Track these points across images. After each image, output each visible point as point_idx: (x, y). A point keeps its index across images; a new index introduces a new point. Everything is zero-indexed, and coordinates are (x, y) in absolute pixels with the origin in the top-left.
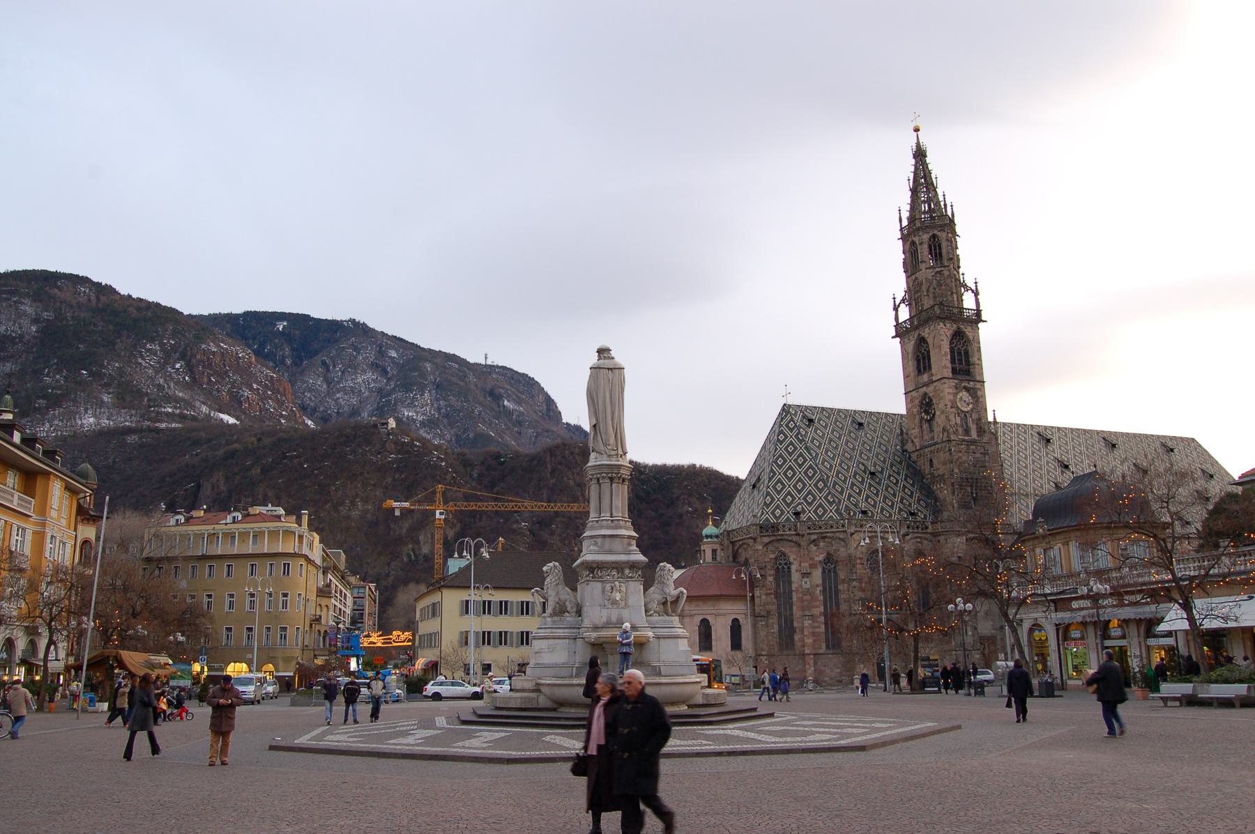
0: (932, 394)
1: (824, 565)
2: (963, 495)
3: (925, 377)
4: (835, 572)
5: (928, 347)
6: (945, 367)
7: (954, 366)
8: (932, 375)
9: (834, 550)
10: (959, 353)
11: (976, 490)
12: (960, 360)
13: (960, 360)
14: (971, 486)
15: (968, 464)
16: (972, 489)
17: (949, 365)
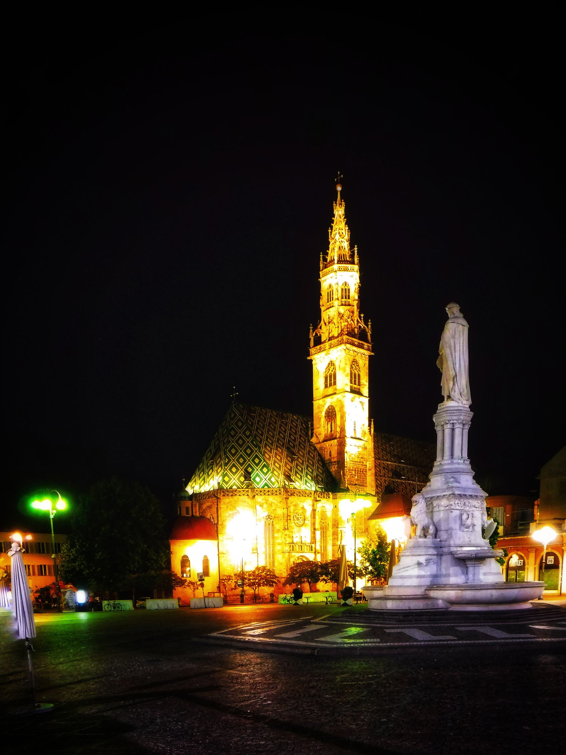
0: (336, 403)
1: (266, 520)
2: (350, 477)
3: (330, 390)
4: (273, 525)
5: (335, 368)
6: (347, 385)
7: (352, 385)
8: (336, 389)
9: (273, 510)
10: (355, 375)
11: (358, 473)
12: (355, 381)
13: (355, 381)
14: (355, 471)
15: (355, 455)
16: (355, 473)
17: (349, 384)
